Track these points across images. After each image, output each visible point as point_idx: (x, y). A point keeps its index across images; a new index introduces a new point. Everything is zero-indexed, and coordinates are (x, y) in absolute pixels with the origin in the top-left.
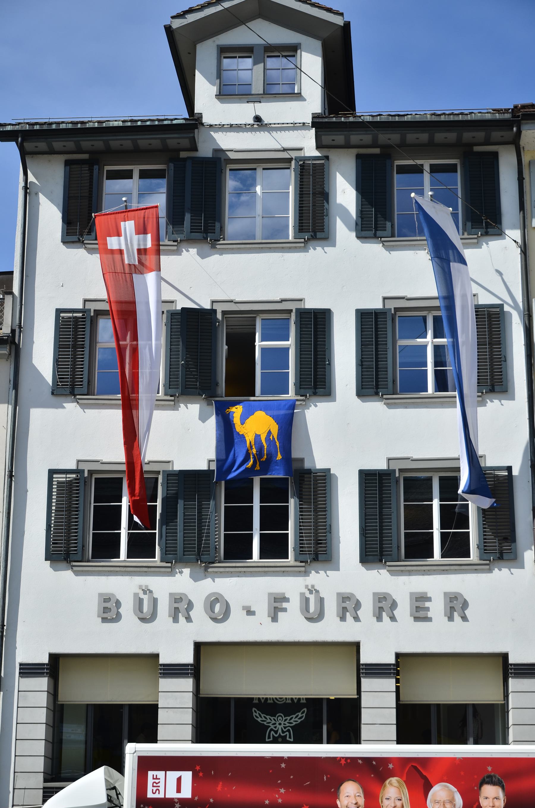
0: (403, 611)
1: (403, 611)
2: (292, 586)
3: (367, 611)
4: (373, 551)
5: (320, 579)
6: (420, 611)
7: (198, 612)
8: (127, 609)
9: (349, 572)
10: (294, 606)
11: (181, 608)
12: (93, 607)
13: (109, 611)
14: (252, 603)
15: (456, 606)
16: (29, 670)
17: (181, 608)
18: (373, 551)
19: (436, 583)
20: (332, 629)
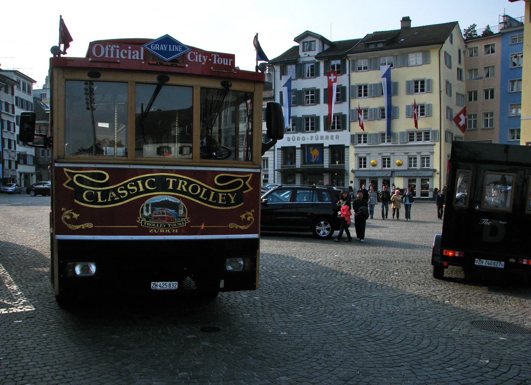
0: (330, 138)
1: (330, 138)
2: (314, 135)
3: (324, 138)
4: (326, 129)
6: (332, 138)
7: (301, 139)
8: (291, 139)
9: (322, 132)
10: (314, 138)
11: (298, 139)
14: (309, 138)
15: (337, 137)
16: (278, 149)
17: (298, 139)
18: (326, 129)
19: (334, 134)
20: (319, 142)
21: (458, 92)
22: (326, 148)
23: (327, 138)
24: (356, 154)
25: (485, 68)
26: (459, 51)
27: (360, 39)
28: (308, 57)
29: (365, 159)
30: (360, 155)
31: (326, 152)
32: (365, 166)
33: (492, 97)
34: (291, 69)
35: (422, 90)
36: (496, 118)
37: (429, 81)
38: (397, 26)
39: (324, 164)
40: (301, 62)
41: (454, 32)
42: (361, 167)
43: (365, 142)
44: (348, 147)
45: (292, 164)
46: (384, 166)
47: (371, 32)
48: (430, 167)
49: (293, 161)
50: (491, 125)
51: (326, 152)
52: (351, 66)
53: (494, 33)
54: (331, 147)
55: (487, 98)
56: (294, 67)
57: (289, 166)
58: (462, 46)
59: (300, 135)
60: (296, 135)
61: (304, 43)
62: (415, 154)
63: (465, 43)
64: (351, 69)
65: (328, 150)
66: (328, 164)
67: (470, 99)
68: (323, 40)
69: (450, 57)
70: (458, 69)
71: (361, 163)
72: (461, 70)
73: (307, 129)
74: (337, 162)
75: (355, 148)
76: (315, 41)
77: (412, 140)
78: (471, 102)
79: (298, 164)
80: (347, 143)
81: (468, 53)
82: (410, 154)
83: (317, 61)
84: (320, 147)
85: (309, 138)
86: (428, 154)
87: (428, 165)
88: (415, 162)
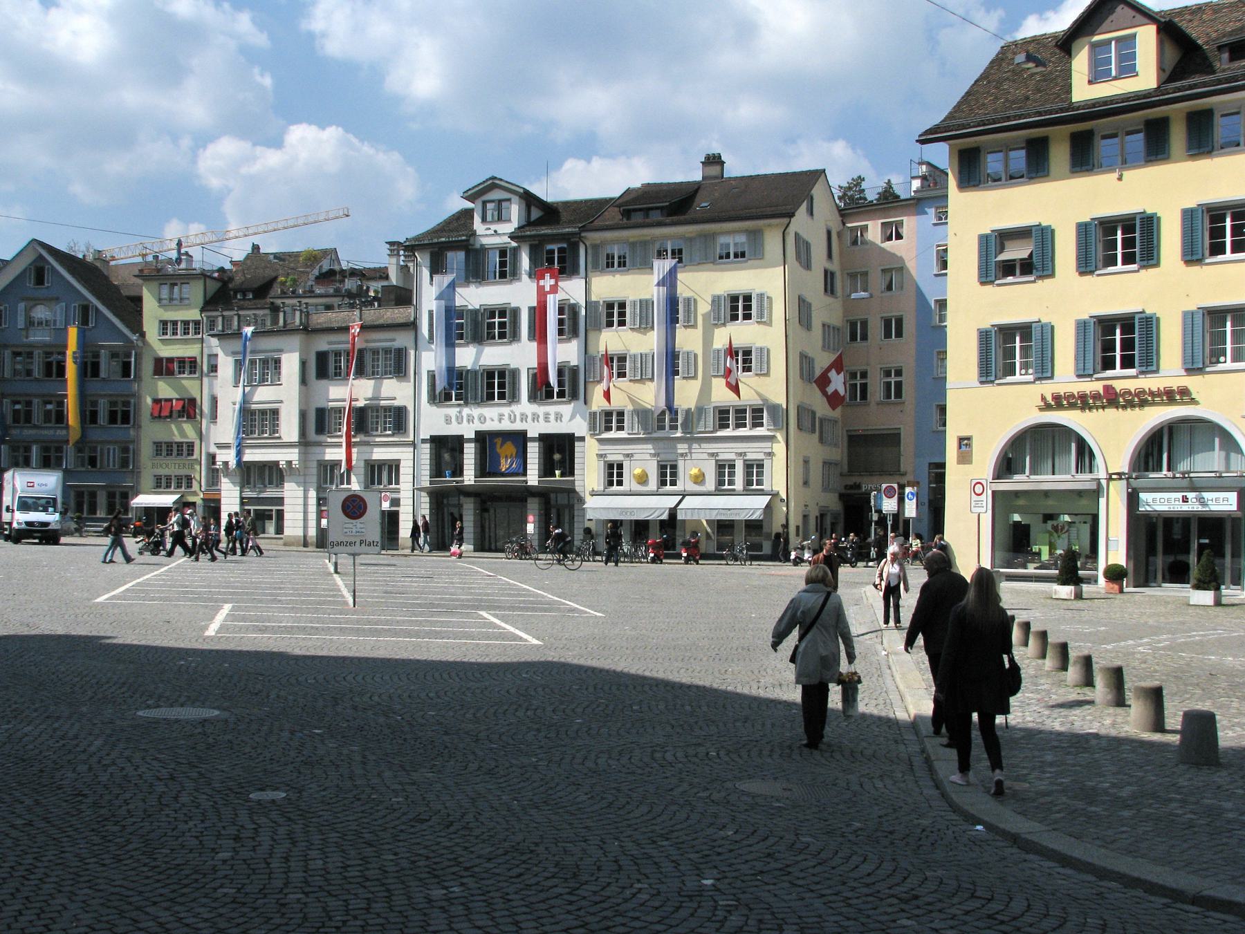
2: (506, 411)
3: (529, 419)
4: (533, 398)
5: (514, 407)
6: (547, 419)
7: (476, 420)
8: (454, 419)
9: (524, 405)
11: (470, 419)
12: (443, 419)
13: (448, 420)
14: (494, 417)
15: (559, 417)
16: (424, 441)
17: (470, 419)
18: (533, 398)
19: (552, 409)
20: (518, 426)
21: (828, 321)
22: (533, 439)
23: (535, 417)
24: (600, 456)
25: (883, 270)
26: (829, 233)
27: (611, 199)
28: (494, 234)
29: (620, 466)
30: (610, 458)
31: (533, 451)
32: (620, 483)
33: (899, 334)
34: (456, 258)
35: (747, 317)
36: (907, 380)
37: (761, 296)
38: (696, 175)
39: (529, 478)
40: (478, 246)
41: (817, 191)
42: (611, 483)
43: (620, 428)
44: (582, 439)
45: (454, 474)
46: (663, 483)
47: (637, 185)
48: (766, 487)
49: (458, 471)
50: (899, 394)
51: (533, 451)
52: (590, 259)
53: (902, 197)
54: (545, 439)
55: (888, 335)
56: (461, 255)
57: (448, 480)
58: (835, 223)
59: (476, 411)
60: (466, 411)
61: (484, 203)
62: (732, 456)
63: (842, 216)
64: (589, 266)
65: (536, 444)
66: (536, 478)
67: (853, 338)
68: (529, 199)
69: (808, 245)
70: (826, 271)
71: (611, 475)
72: (832, 274)
73: (490, 397)
74: (557, 472)
75: (598, 440)
76: (509, 200)
77: (724, 426)
78: (855, 344)
79: (469, 477)
80: (578, 426)
81: (848, 239)
82: (721, 457)
83: (514, 244)
84: (520, 438)
85: (494, 417)
86: (761, 456)
87: (759, 483)
88: (732, 474)
